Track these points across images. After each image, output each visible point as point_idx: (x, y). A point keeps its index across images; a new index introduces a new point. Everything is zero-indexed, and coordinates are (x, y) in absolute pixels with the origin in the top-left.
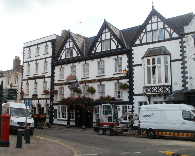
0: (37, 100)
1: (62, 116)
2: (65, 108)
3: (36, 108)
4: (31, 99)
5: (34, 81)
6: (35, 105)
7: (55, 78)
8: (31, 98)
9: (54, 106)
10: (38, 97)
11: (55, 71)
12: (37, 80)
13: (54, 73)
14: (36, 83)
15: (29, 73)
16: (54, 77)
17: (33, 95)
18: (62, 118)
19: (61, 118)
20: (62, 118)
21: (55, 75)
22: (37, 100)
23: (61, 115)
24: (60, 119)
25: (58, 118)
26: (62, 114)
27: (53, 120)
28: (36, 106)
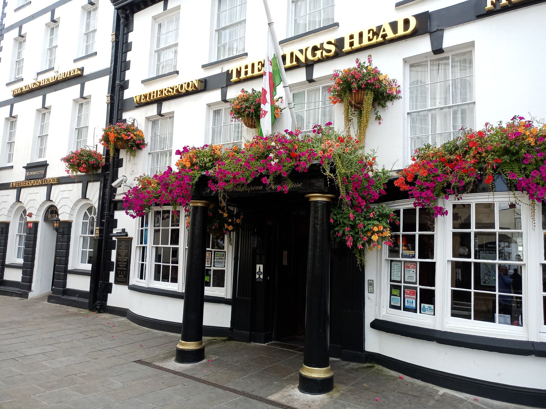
0: (44, 189)
1: (157, 268)
2: (176, 222)
3: (36, 224)
4: (19, 187)
5: (36, 102)
6: (34, 212)
7: (129, 75)
8: (18, 183)
9: (119, 215)
10: (52, 173)
11: (131, 37)
12: (52, 97)
13: (128, 47)
14: (45, 109)
15: (19, 70)
16: (126, 66)
17: (29, 167)
18: (157, 278)
19: (150, 282)
20: (157, 278)
21: (130, 56)
22: (44, 189)
23: (150, 263)
24: (143, 283)
25: (134, 279)
26: (158, 258)
27: (108, 289)
28: (38, 216)
